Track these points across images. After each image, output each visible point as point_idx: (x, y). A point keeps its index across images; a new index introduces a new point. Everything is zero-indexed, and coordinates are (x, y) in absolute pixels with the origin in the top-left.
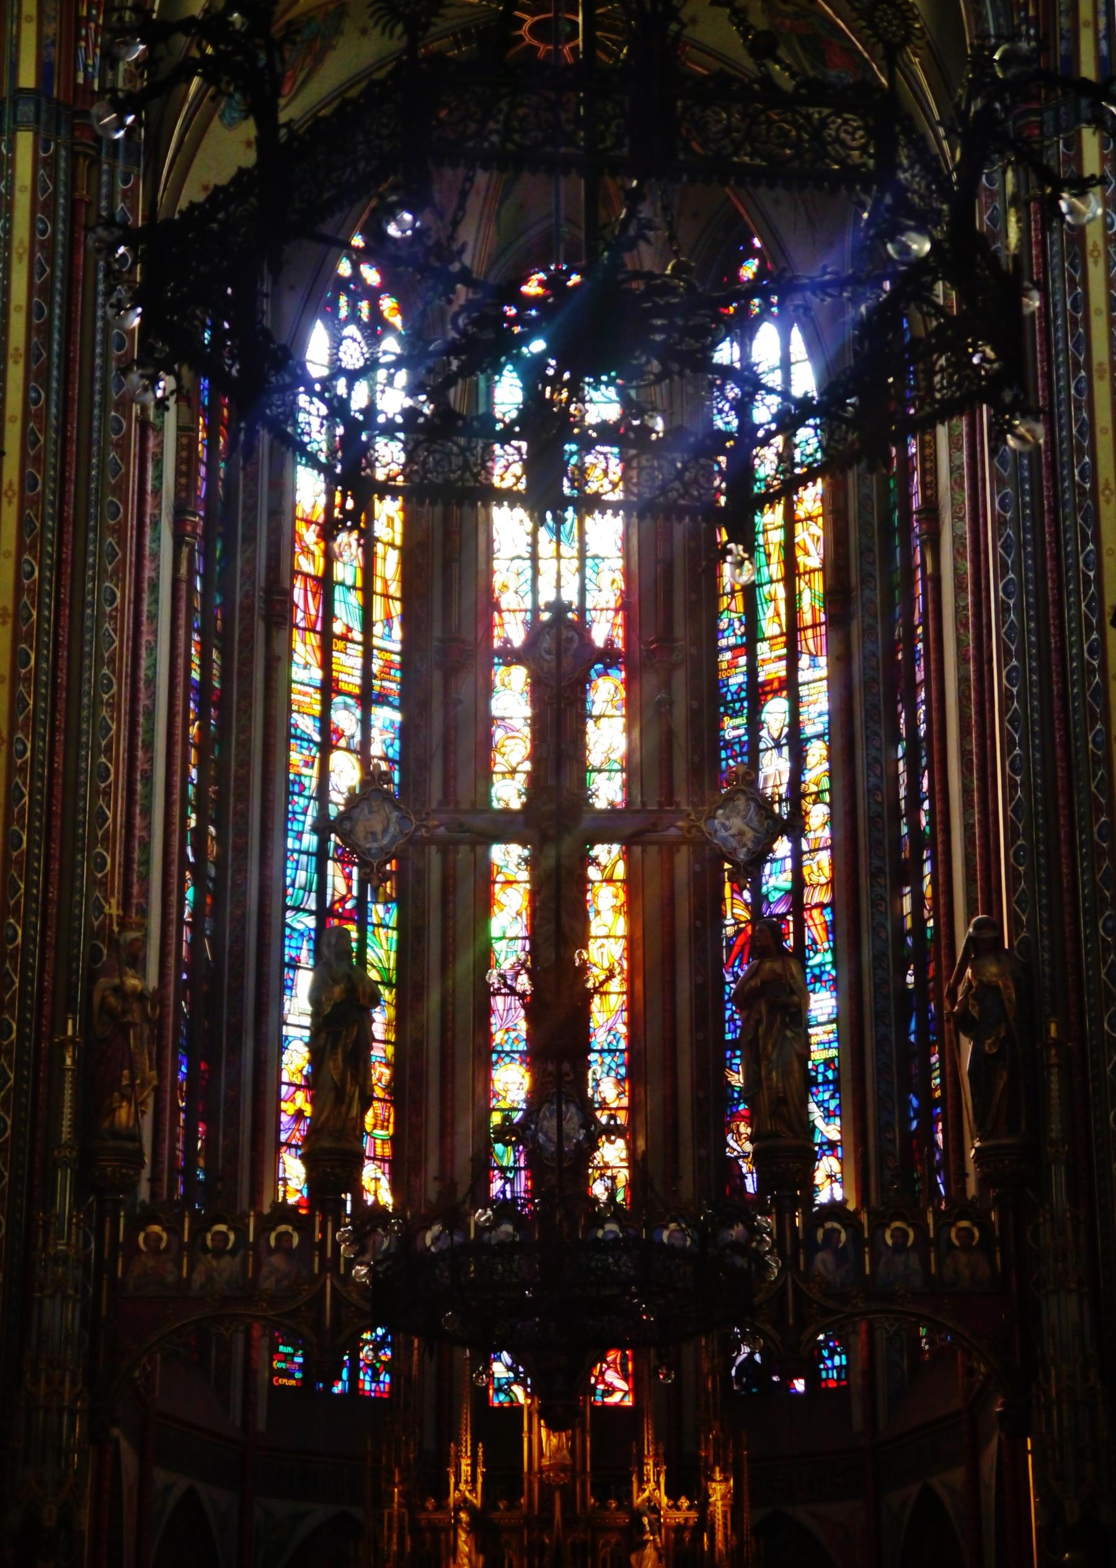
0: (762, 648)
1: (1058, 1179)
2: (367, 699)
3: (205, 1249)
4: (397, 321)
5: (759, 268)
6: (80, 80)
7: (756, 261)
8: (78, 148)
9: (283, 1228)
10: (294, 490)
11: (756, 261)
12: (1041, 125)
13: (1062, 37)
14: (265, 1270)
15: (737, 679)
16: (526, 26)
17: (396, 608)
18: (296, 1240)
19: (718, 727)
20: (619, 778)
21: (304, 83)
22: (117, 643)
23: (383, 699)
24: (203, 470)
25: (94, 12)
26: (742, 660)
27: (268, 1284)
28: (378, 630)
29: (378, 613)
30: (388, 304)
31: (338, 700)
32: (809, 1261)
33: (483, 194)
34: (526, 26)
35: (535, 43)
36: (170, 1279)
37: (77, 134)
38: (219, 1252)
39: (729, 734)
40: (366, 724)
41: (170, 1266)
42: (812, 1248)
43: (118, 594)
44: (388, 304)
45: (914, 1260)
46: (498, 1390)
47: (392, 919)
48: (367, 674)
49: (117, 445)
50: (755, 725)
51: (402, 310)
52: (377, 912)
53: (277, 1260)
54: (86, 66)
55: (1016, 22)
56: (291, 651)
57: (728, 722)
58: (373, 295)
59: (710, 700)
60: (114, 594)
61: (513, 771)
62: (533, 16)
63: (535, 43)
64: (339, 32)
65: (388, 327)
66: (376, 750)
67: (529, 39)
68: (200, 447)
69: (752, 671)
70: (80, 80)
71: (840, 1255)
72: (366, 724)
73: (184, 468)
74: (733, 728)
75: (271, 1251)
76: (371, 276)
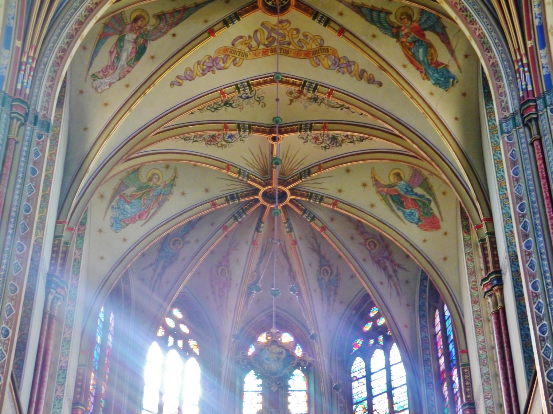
4: (197, 351)
5: (372, 325)
6: (19, 86)
7: (371, 323)
8: (13, 115)
11: (371, 323)
12: (536, 107)
13: (543, 67)
16: (261, 193)
21: (153, 214)
22: (6, 358)
24: (92, 399)
25: (30, 61)
30: (192, 343)
33: (239, 285)
34: (261, 193)
35: (265, 203)
37: (14, 109)
43: (11, 332)
44: (192, 343)
49: (19, 257)
51: (198, 346)
54: (22, 83)
55: (516, 68)
58: (185, 338)
60: (8, 331)
62: (264, 187)
63: (265, 203)
64: (171, 193)
67: (262, 202)
68: (91, 387)
70: (19, 86)
73: (80, 384)
76: (184, 329)
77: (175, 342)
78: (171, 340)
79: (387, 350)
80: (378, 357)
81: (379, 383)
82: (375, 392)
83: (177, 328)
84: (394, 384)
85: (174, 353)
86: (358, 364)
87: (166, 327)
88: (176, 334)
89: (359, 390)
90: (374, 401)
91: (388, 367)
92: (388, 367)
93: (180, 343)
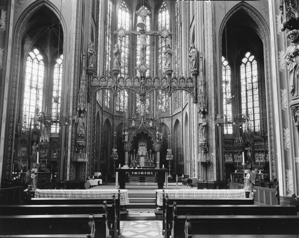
0: (163, 43)
1: (201, 73)
2: (125, 47)
3: (101, 81)
4: (128, 11)
9: (111, 79)
10: (118, 20)
14: (108, 83)
15: (160, 46)
17: (128, 39)
18: (112, 80)
19: (158, 51)
20: (149, 56)
23: (127, 48)
26: (161, 44)
27: (109, 85)
28: (126, 41)
29: (126, 39)
30: (127, 9)
31: (122, 47)
32: (172, 83)
36: (97, 84)
38: (103, 81)
39: (159, 51)
40: (125, 50)
41: (97, 83)
42: (172, 82)
45: (184, 83)
46: (137, 112)
47: (127, 68)
48: (125, 45)
50: (162, 50)
52: (126, 68)
53: (110, 82)
56: (117, 41)
57: (159, 50)
59: (158, 49)
61: (139, 55)
65: (127, 11)
66: (126, 52)
69: (162, 46)
71: (175, 82)
72: (125, 50)
74: (160, 51)
75: (109, 81)
76: (125, 6)
77: (124, 9)
78: (123, 9)
79: (166, 11)
80: (164, 12)
81: (164, 19)
82: (163, 21)
83: (124, 6)
84: (167, 19)
85: (123, 11)
86: (160, 14)
87: (122, 6)
88: (124, 7)
89: (160, 20)
90: (163, 22)
91: (166, 15)
92: (166, 15)
93: (125, 9)
